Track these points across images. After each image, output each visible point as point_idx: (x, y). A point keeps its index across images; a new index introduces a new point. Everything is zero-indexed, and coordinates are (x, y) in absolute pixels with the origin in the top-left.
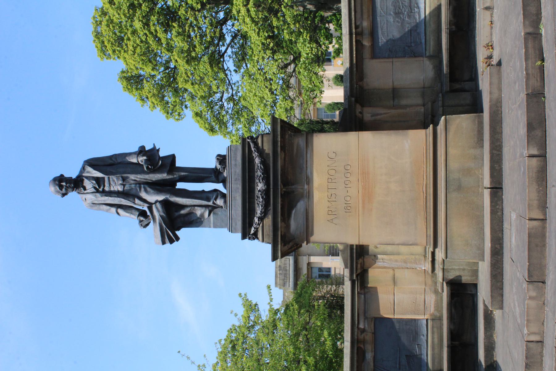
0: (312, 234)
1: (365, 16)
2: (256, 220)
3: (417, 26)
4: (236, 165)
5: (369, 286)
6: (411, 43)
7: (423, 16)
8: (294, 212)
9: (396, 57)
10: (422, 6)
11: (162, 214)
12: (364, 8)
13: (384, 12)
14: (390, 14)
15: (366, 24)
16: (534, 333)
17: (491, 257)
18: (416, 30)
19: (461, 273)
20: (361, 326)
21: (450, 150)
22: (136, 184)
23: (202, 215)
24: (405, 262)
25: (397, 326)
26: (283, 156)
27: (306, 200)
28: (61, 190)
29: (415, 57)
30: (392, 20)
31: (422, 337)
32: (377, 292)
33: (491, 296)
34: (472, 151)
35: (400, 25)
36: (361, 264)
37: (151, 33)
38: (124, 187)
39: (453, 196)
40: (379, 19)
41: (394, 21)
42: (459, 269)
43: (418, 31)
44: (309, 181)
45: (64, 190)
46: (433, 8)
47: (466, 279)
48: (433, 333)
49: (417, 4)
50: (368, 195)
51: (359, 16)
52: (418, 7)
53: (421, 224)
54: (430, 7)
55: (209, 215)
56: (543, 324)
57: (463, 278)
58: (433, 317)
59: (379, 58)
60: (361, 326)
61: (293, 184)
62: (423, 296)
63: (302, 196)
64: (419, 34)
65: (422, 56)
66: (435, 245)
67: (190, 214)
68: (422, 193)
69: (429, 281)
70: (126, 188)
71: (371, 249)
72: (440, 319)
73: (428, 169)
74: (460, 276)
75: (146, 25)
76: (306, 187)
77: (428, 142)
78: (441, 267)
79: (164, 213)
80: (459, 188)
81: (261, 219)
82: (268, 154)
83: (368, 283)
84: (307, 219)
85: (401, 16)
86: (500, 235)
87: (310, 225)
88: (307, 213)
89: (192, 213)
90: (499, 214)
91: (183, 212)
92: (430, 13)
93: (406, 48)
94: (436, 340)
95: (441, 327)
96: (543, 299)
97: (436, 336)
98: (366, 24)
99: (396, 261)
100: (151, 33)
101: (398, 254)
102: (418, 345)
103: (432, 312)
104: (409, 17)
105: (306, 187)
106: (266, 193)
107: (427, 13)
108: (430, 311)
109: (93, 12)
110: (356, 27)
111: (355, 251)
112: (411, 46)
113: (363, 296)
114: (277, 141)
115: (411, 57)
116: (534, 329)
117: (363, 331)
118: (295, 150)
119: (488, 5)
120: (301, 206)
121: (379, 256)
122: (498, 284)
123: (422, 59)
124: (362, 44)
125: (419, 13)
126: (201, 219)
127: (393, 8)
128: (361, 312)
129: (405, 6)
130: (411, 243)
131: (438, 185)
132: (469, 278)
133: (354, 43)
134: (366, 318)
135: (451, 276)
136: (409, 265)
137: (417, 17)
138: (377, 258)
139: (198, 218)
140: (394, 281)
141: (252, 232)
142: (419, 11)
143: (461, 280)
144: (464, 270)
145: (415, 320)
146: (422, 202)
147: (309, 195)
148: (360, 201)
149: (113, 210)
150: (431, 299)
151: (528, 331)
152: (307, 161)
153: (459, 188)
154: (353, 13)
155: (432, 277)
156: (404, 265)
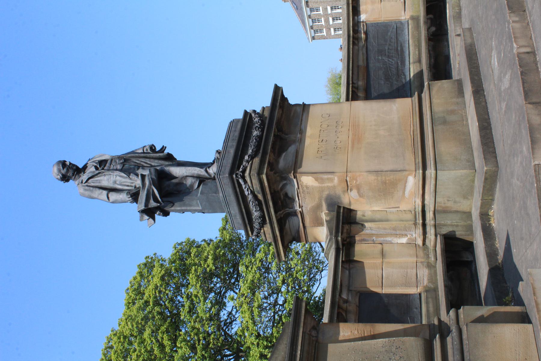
0: (300, 167)
1: (361, 78)
2: (246, 157)
3: (404, 86)
4: (235, 131)
5: (355, 259)
7: (408, 79)
8: (284, 154)
10: (407, 74)
11: (154, 177)
12: (360, 73)
15: (361, 83)
16: (525, 46)
17: (480, 131)
19: (455, 229)
20: (344, 296)
21: (434, 101)
22: (135, 166)
23: (192, 186)
24: (394, 229)
25: (386, 300)
26: (281, 112)
27: (297, 144)
28: (63, 168)
30: (383, 82)
31: (415, 310)
32: (363, 268)
33: (484, 158)
34: (455, 100)
36: (347, 230)
37: (158, 341)
38: (123, 166)
39: (439, 128)
40: (372, 83)
42: (452, 224)
44: (302, 132)
45: (65, 170)
46: (416, 72)
47: (460, 233)
48: (427, 303)
50: (357, 139)
51: (355, 77)
52: (405, 75)
53: (409, 156)
54: (414, 72)
55: (199, 186)
56: (531, 38)
57: (457, 233)
58: (427, 289)
60: (344, 296)
61: (287, 135)
62: (415, 271)
63: (294, 142)
66: (424, 168)
67: (180, 184)
68: (409, 136)
69: (421, 253)
70: (124, 168)
71: (359, 215)
72: (435, 290)
73: (415, 121)
74: (454, 232)
75: (154, 332)
76: (299, 135)
77: (414, 105)
78: (432, 222)
79: (155, 176)
80: (445, 122)
81: (252, 157)
82: (266, 117)
83: (354, 256)
84: (297, 157)
86: (486, 117)
87: (299, 162)
88: (295, 163)
89: (183, 183)
90: (483, 104)
91: (174, 181)
92: (414, 76)
94: (431, 309)
95: (436, 297)
96: (526, 22)
97: (431, 305)
98: (361, 83)
99: (385, 229)
100: (158, 341)
101: (387, 220)
102: (410, 317)
103: (425, 284)
104: (397, 81)
105: (299, 135)
106: (260, 138)
107: (412, 75)
108: (423, 283)
109: (109, 333)
110: (353, 83)
111: (341, 214)
113: (347, 272)
114: (277, 100)
116: (522, 42)
117: (346, 301)
118: (292, 114)
119: (458, 33)
120: (292, 149)
121: (367, 225)
122: (491, 150)
124: (357, 95)
125: (405, 78)
126: (189, 189)
128: (345, 283)
130: (399, 170)
131: (425, 126)
132: (463, 233)
133: (351, 93)
134: (349, 290)
135: (445, 231)
136: (398, 232)
137: (404, 81)
138: (365, 227)
139: (188, 188)
140: (383, 254)
141: (241, 170)
143: (455, 235)
144: (457, 226)
145: (406, 295)
146: (409, 142)
147: (301, 141)
148: (350, 143)
149: (105, 192)
150: (424, 273)
151: (517, 45)
152: (302, 120)
153: (445, 122)
154: (351, 72)
155: (424, 250)
156: (394, 232)
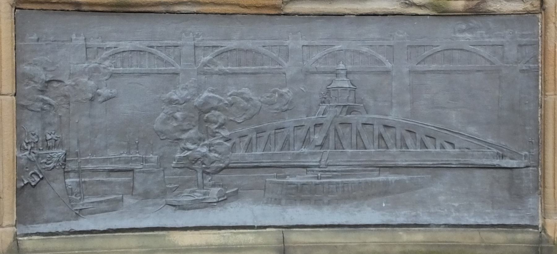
6: (79, 172)
9: (20, 107)
13: (210, 62)
14: (200, 89)
18: (131, 190)
29: (19, 191)
35: (157, 125)
41: (171, 102)
43: (129, 200)
49: (236, 195)
59: (17, 37)
64: (114, 206)
65: (21, 220)
85: (192, 133)
93: (59, 152)
112: (66, 173)
115: (20, 170)
123: (10, 218)
127: (227, 100)
129: (233, 149)
142: (210, 205)
